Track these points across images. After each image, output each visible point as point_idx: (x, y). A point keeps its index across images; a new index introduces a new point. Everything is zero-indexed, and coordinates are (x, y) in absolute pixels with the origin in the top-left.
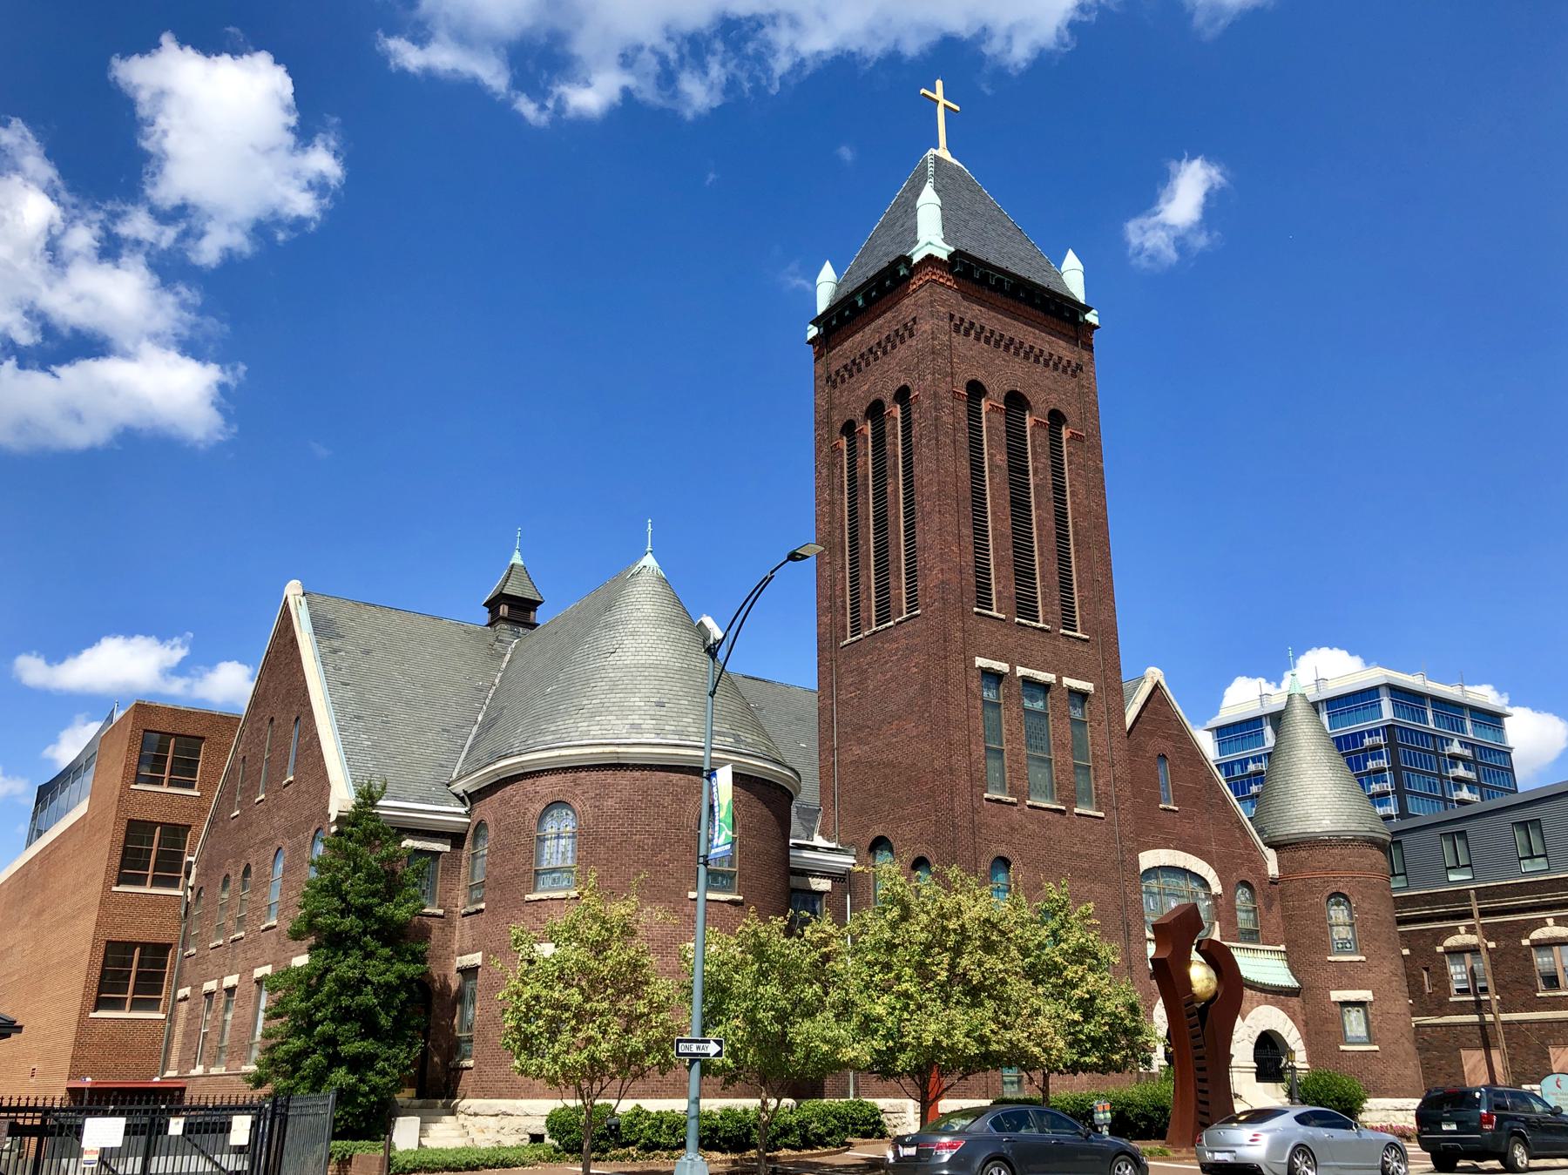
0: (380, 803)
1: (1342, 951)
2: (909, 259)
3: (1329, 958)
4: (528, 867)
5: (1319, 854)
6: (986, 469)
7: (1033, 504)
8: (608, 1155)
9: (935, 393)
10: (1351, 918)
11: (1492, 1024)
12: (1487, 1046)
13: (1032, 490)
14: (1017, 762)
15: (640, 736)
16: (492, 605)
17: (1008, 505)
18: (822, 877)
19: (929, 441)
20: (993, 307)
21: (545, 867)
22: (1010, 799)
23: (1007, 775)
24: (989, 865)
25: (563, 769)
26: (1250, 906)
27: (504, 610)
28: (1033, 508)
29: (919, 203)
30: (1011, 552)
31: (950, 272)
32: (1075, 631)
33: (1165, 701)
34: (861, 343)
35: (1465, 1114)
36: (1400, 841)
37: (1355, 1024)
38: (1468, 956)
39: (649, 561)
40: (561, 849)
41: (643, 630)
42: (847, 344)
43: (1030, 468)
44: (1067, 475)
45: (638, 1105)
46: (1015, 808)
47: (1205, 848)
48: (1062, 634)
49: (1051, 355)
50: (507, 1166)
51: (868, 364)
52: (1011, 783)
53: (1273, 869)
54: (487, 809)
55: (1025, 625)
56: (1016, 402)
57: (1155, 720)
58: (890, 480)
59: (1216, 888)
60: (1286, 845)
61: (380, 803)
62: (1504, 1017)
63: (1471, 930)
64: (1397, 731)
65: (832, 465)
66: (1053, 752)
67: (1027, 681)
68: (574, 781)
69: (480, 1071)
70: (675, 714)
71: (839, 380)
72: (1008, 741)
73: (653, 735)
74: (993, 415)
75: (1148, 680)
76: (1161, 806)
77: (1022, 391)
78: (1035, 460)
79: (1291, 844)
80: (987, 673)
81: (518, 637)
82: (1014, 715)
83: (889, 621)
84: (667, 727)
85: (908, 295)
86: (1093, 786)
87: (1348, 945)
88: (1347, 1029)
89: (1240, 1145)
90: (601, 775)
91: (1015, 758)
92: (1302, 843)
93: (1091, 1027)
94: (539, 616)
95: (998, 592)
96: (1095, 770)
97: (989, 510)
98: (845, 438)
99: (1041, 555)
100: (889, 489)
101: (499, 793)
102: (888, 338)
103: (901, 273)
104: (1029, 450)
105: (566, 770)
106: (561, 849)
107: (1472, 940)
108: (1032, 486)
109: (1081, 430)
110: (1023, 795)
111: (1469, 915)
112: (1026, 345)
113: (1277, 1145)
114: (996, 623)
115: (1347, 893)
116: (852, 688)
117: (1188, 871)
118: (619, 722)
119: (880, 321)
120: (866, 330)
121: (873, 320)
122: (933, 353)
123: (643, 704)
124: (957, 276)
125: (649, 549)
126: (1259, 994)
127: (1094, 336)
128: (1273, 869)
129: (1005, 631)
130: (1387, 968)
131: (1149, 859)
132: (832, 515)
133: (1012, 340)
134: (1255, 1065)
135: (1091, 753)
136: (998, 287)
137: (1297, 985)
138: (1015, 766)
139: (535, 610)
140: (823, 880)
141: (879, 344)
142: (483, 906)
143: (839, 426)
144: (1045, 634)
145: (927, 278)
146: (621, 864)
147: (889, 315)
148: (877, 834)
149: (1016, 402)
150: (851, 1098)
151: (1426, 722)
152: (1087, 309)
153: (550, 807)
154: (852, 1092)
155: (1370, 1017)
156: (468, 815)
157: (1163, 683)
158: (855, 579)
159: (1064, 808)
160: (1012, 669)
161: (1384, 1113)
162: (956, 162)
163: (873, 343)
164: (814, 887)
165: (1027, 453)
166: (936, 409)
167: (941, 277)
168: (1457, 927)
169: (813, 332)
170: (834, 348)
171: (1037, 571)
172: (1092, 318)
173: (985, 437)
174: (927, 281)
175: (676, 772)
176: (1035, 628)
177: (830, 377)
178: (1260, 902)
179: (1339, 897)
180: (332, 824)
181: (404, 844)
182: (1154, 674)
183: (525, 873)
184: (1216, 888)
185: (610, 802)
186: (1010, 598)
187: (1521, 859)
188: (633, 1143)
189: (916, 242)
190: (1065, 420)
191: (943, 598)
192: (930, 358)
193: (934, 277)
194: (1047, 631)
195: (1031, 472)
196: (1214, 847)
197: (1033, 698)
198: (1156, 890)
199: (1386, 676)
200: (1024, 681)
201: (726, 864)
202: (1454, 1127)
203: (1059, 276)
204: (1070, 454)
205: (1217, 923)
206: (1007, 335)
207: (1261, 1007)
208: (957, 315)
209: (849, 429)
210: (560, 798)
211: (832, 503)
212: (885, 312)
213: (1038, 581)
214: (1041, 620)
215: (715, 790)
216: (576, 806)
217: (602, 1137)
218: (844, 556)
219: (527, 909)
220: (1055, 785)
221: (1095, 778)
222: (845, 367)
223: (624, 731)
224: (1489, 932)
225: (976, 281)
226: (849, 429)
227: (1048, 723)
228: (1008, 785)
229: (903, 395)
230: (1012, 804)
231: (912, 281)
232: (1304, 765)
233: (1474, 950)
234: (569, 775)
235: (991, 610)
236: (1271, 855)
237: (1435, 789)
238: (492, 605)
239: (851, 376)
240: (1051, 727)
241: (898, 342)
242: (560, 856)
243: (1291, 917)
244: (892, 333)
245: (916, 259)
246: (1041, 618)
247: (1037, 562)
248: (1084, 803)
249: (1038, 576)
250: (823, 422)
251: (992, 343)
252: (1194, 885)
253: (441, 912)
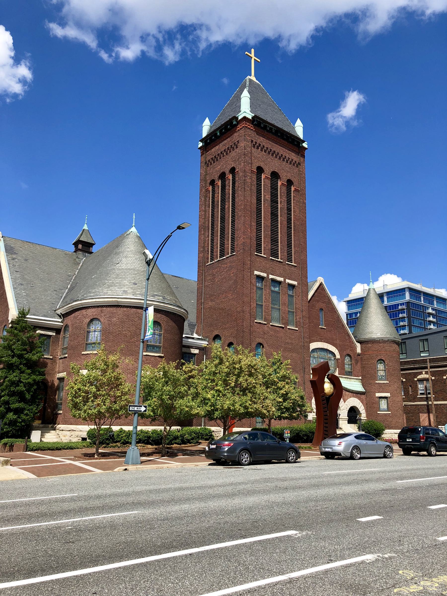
0: (28, 316)
1: (381, 380)
2: (237, 118)
3: (376, 382)
4: (83, 342)
5: (376, 346)
6: (262, 201)
7: (279, 215)
8: (109, 445)
9: (244, 170)
10: (385, 368)
11: (431, 405)
12: (429, 412)
13: (279, 209)
14: (268, 309)
15: (126, 295)
16: (76, 244)
17: (269, 214)
18: (195, 348)
19: (241, 188)
20: (268, 139)
21: (90, 342)
22: (264, 323)
23: (264, 314)
24: (255, 346)
25: (97, 306)
26: (350, 363)
27: (80, 246)
28: (279, 216)
29: (242, 96)
30: (270, 232)
31: (252, 124)
32: (292, 263)
33: (324, 290)
34: (218, 150)
35: (415, 436)
36: (405, 342)
37: (383, 405)
38: (425, 382)
39: (133, 229)
40: (96, 336)
41: (129, 255)
42: (213, 150)
43: (279, 201)
44: (292, 204)
45: (121, 428)
46: (266, 326)
47: (335, 342)
48: (287, 264)
49: (289, 158)
50: (72, 449)
51: (220, 158)
52: (265, 317)
53: (359, 350)
54: (69, 320)
55: (273, 260)
56: (275, 176)
57: (319, 296)
58: (227, 203)
59: (338, 356)
60: (364, 342)
61: (28, 316)
62: (435, 403)
63: (426, 373)
64: (410, 304)
65: (206, 197)
66: (281, 306)
67: (273, 280)
68: (101, 311)
69: (64, 415)
70: (140, 288)
71: (209, 164)
72: (265, 301)
73: (132, 295)
74: (266, 180)
75: (318, 281)
76: (320, 327)
77: (277, 171)
78: (281, 198)
79: (366, 342)
80: (258, 277)
81: (85, 257)
82: (268, 292)
83: (224, 256)
84: (137, 292)
85: (236, 132)
86: (295, 319)
87: (383, 377)
88: (381, 406)
89: (334, 446)
90: (111, 309)
92: (370, 341)
93: (286, 404)
94: (94, 249)
95: (264, 247)
96: (296, 313)
97: (263, 216)
98: (211, 186)
99: (281, 234)
100: (226, 207)
101: (73, 314)
102: (228, 148)
103: (234, 123)
104: (279, 194)
105: (98, 307)
106: (96, 336)
107: (427, 376)
108: (279, 208)
109: (299, 188)
110: (269, 321)
111: (426, 368)
112: (280, 154)
113: (347, 446)
114: (263, 259)
115: (384, 359)
116: (210, 281)
117: (328, 350)
118: (119, 289)
119: (225, 141)
120: (220, 145)
121: (223, 141)
122: (244, 155)
123: (128, 283)
124: (255, 125)
125: (134, 225)
126: (351, 394)
127: (305, 152)
128: (359, 350)
130: (396, 385)
131: (313, 346)
132: (205, 216)
133: (274, 152)
134: (348, 418)
135: (295, 307)
136: (270, 131)
137: (365, 391)
138: (267, 311)
139: (92, 247)
140: (196, 350)
141: (225, 150)
142: (67, 355)
143: (209, 181)
144: (281, 263)
145: (243, 125)
146: (118, 342)
147: (229, 139)
148: (216, 334)
149: (275, 176)
150: (203, 427)
151: (421, 301)
152: (303, 142)
153: (92, 320)
154: (203, 424)
155: (389, 402)
156: (62, 322)
157: (323, 283)
158: (212, 240)
159: (283, 326)
160: (268, 275)
161: (391, 434)
162: (257, 82)
163: (223, 150)
164: (192, 352)
165: (278, 195)
166: (245, 177)
167: (249, 125)
168: (422, 372)
169: (201, 144)
170: (208, 151)
171: (279, 240)
172: (305, 145)
173: (262, 188)
174: (243, 127)
175: (140, 309)
176: (277, 261)
177: (206, 162)
178: (353, 362)
179: (381, 361)
180: (10, 324)
181: (37, 332)
182: (320, 279)
183: (82, 344)
184: (338, 356)
185: (114, 319)
186: (268, 249)
187: (445, 349)
188: (119, 442)
189: (240, 111)
190: (293, 184)
191: (243, 249)
192: (243, 157)
193: (246, 125)
194: (281, 262)
195: (279, 203)
196: (338, 342)
197: (275, 287)
198: (316, 356)
199: (408, 284)
200: (272, 280)
201: (158, 343)
202: (411, 440)
203: (294, 128)
204: (294, 196)
205: (337, 369)
206: (273, 150)
207: (351, 398)
208: (254, 141)
209: (212, 183)
210: (96, 317)
211: (205, 211)
212: (227, 138)
213: (279, 243)
214: (280, 258)
215: (147, 315)
216: (102, 320)
217: (107, 439)
218: (209, 231)
219: (83, 357)
220: (281, 318)
221: (296, 316)
222: (212, 159)
223: (121, 293)
224: (433, 374)
225: (262, 128)
226: (212, 183)
227: (280, 295)
228: (264, 318)
229: (233, 171)
230: (265, 324)
231: (238, 127)
232: (372, 314)
233: (427, 380)
234: (99, 308)
235: (261, 254)
236: (358, 345)
237: (422, 325)
238: (76, 244)
239: (214, 162)
240: (281, 297)
241: (232, 150)
242: (95, 338)
243: (364, 367)
244: (230, 146)
245: (240, 118)
246: (279, 257)
247: (279, 237)
248: (291, 325)
249: (279, 242)
250: (203, 180)
251: (267, 152)
252: (330, 355)
253: (51, 357)
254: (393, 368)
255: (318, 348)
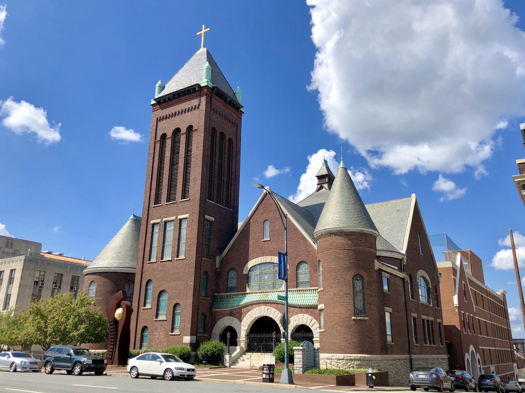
20: (171, 105)
46: (156, 264)
57: (264, 207)
91: (158, 248)
126: (298, 309)
129: (161, 209)
136: (169, 99)
207: (297, 315)
254: (329, 269)
255: (259, 264)
